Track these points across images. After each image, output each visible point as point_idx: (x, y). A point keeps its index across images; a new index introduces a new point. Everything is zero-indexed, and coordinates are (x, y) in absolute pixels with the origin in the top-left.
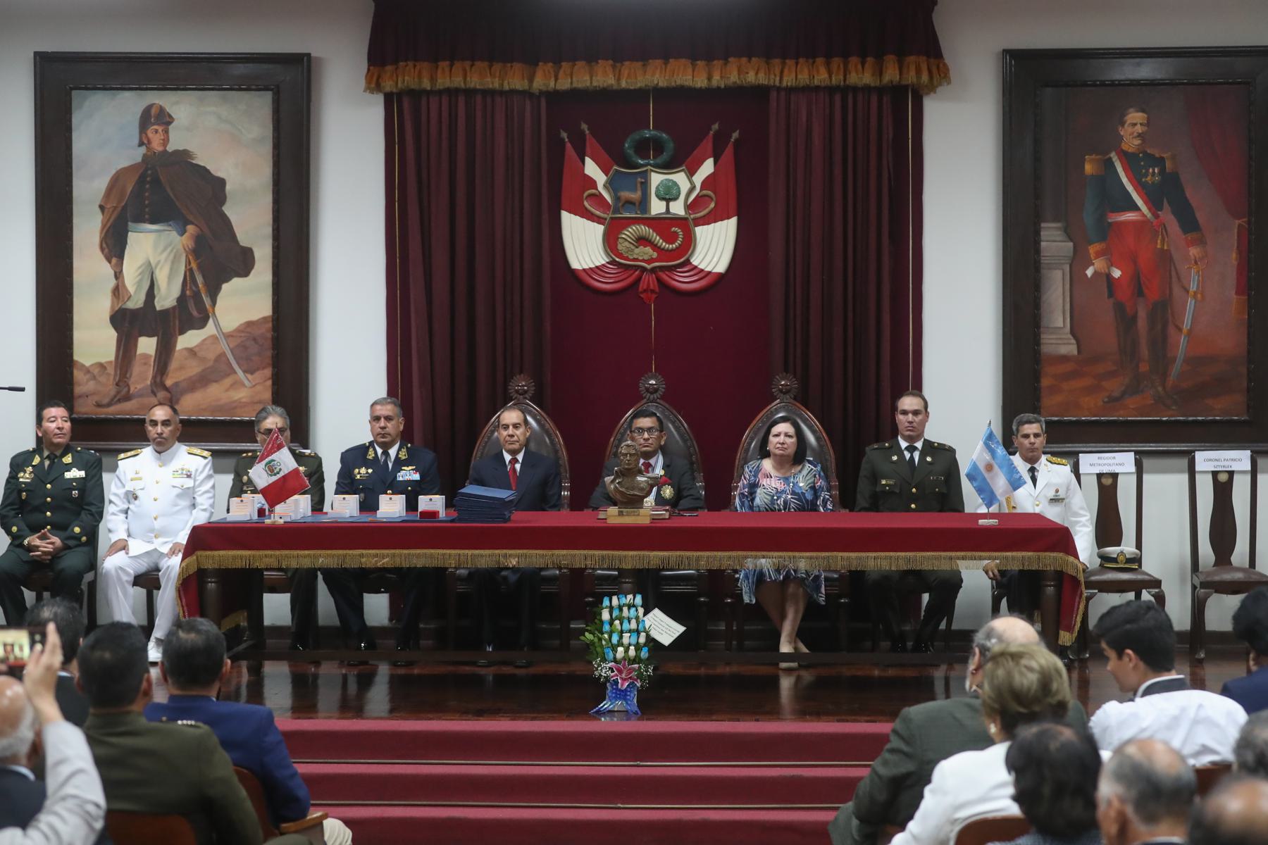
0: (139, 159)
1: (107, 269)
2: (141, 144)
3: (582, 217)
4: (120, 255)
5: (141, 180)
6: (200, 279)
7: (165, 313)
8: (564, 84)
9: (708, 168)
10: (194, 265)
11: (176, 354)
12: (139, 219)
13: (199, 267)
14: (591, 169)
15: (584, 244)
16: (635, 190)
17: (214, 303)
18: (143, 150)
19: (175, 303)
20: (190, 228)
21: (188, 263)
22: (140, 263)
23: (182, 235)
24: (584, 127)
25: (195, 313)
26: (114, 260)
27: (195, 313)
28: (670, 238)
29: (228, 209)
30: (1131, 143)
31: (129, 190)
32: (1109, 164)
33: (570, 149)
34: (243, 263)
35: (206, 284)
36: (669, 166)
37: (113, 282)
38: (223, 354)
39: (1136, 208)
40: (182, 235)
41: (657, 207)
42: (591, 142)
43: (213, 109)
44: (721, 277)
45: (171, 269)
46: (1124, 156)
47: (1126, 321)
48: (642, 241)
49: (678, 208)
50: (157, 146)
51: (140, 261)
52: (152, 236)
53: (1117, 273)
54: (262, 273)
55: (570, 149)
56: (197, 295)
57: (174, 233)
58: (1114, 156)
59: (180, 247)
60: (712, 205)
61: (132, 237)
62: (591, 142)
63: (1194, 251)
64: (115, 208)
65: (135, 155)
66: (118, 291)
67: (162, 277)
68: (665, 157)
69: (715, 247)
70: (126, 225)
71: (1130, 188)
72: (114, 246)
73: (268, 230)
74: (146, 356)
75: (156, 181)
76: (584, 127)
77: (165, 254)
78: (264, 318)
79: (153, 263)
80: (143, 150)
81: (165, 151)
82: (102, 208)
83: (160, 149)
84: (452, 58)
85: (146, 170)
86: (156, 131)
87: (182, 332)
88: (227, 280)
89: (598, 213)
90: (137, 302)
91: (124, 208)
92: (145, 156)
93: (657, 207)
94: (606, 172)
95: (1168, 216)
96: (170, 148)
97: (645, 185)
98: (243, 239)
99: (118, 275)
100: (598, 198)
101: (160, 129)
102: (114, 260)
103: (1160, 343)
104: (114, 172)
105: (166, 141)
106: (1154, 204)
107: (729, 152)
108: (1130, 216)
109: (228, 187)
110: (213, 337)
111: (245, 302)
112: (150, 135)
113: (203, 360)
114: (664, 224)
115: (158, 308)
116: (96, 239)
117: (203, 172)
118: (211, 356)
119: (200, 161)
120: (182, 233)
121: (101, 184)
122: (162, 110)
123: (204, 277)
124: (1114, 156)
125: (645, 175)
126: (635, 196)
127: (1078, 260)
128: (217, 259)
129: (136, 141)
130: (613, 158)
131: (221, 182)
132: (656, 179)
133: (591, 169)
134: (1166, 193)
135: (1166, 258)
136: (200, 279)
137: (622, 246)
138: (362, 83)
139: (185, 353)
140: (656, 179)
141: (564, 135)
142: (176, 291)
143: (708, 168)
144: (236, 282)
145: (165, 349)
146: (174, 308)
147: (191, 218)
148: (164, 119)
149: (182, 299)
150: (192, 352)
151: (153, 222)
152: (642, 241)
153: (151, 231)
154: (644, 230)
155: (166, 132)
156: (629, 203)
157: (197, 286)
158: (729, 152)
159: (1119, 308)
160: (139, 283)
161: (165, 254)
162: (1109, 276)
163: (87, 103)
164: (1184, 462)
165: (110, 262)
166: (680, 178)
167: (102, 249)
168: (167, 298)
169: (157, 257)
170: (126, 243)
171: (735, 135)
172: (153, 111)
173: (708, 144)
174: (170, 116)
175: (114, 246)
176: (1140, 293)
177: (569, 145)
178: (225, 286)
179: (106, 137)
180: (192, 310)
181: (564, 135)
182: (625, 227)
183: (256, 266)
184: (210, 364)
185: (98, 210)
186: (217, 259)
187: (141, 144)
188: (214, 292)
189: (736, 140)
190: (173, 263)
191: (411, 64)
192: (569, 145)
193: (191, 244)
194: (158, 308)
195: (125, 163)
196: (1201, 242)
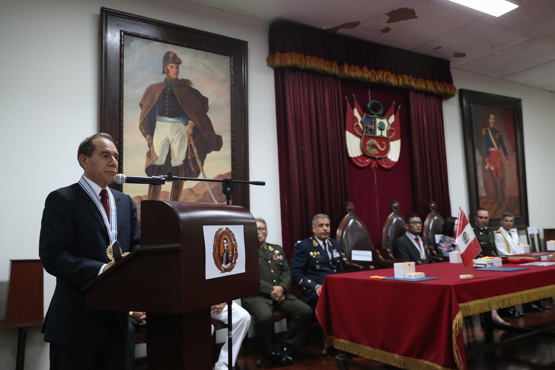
0: (163, 81)
1: (143, 141)
2: (164, 72)
3: (353, 134)
4: (152, 134)
5: (164, 92)
7: (177, 168)
8: (353, 74)
9: (392, 119)
10: (192, 143)
11: (183, 192)
12: (163, 114)
13: (196, 144)
14: (356, 113)
15: (354, 146)
16: (372, 124)
17: (203, 164)
18: (165, 76)
19: (182, 163)
20: (190, 122)
22: (163, 139)
23: (186, 125)
24: (354, 95)
25: (193, 169)
26: (148, 136)
27: (193, 169)
28: (382, 147)
29: (210, 114)
30: (492, 125)
31: (157, 96)
32: (487, 131)
33: (349, 105)
34: (217, 144)
35: (199, 153)
36: (382, 116)
37: (147, 149)
38: (208, 192)
39: (494, 147)
40: (186, 125)
41: (378, 133)
42: (356, 103)
43: (202, 60)
44: (396, 163)
45: (180, 144)
46: (491, 129)
47: (496, 185)
48: (374, 146)
49: (385, 134)
53: (492, 168)
54: (226, 150)
55: (349, 105)
56: (194, 159)
57: (182, 125)
58: (488, 129)
59: (185, 132)
60: (394, 134)
61: (158, 124)
62: (356, 103)
63: (507, 162)
64: (149, 107)
65: (162, 78)
66: (150, 154)
68: (381, 112)
69: (394, 152)
70: (155, 117)
71: (493, 140)
72: (148, 128)
73: (229, 127)
74: (166, 193)
75: (172, 94)
76: (354, 95)
77: (177, 135)
78: (228, 173)
79: (170, 141)
80: (165, 76)
81: (177, 79)
82: (141, 105)
83: (175, 77)
84: (312, 56)
85: (166, 87)
86: (172, 67)
89: (358, 133)
90: (161, 161)
91: (154, 107)
92: (166, 80)
93: (378, 133)
94: (362, 116)
95: (501, 150)
96: (180, 77)
97: (375, 122)
98: (217, 130)
99: (150, 145)
100: (358, 126)
101: (174, 66)
102: (148, 136)
103: (503, 192)
104: (148, 86)
105: (177, 73)
106: (498, 146)
107: (398, 112)
108: (493, 149)
109: (209, 103)
111: (217, 164)
112: (169, 67)
113: (197, 195)
114: (380, 139)
115: (173, 165)
116: (138, 123)
117: (196, 93)
118: (201, 193)
119: (196, 86)
120: (186, 124)
121: (141, 92)
122: (175, 56)
123: (198, 150)
124: (488, 129)
125: (374, 118)
126: (372, 127)
127: (484, 164)
128: (204, 141)
129: (161, 70)
130: (364, 110)
131: (205, 100)
132: (378, 121)
133: (356, 113)
134: (500, 142)
135: (502, 164)
137: (368, 148)
138: (265, 63)
139: (188, 191)
140: (378, 121)
141: (346, 98)
142: (183, 157)
143: (392, 119)
144: (214, 153)
145: (177, 189)
146: (182, 166)
147: (190, 116)
149: (186, 161)
150: (191, 190)
151: (170, 117)
152: (374, 146)
154: (375, 142)
155: (178, 68)
156: (371, 130)
157: (194, 154)
158: (398, 112)
159: (494, 180)
160: (162, 151)
161: (177, 135)
162: (490, 169)
164: (524, 231)
165: (145, 137)
166: (385, 121)
167: (141, 130)
168: (178, 160)
169: (171, 135)
170: (155, 127)
171: (399, 107)
172: (171, 56)
173: (392, 109)
174: (180, 60)
175: (148, 128)
176: (497, 175)
177: (348, 103)
178: (208, 155)
179: (144, 66)
180: (191, 168)
181: (346, 98)
182: (370, 139)
183: (223, 146)
184: (201, 197)
185: (139, 106)
186: (204, 141)
187: (164, 72)
188: (203, 159)
189: (401, 109)
190: (181, 140)
191: (296, 54)
192: (348, 103)
193: (191, 131)
194: (173, 165)
195: (154, 82)
196: (508, 159)
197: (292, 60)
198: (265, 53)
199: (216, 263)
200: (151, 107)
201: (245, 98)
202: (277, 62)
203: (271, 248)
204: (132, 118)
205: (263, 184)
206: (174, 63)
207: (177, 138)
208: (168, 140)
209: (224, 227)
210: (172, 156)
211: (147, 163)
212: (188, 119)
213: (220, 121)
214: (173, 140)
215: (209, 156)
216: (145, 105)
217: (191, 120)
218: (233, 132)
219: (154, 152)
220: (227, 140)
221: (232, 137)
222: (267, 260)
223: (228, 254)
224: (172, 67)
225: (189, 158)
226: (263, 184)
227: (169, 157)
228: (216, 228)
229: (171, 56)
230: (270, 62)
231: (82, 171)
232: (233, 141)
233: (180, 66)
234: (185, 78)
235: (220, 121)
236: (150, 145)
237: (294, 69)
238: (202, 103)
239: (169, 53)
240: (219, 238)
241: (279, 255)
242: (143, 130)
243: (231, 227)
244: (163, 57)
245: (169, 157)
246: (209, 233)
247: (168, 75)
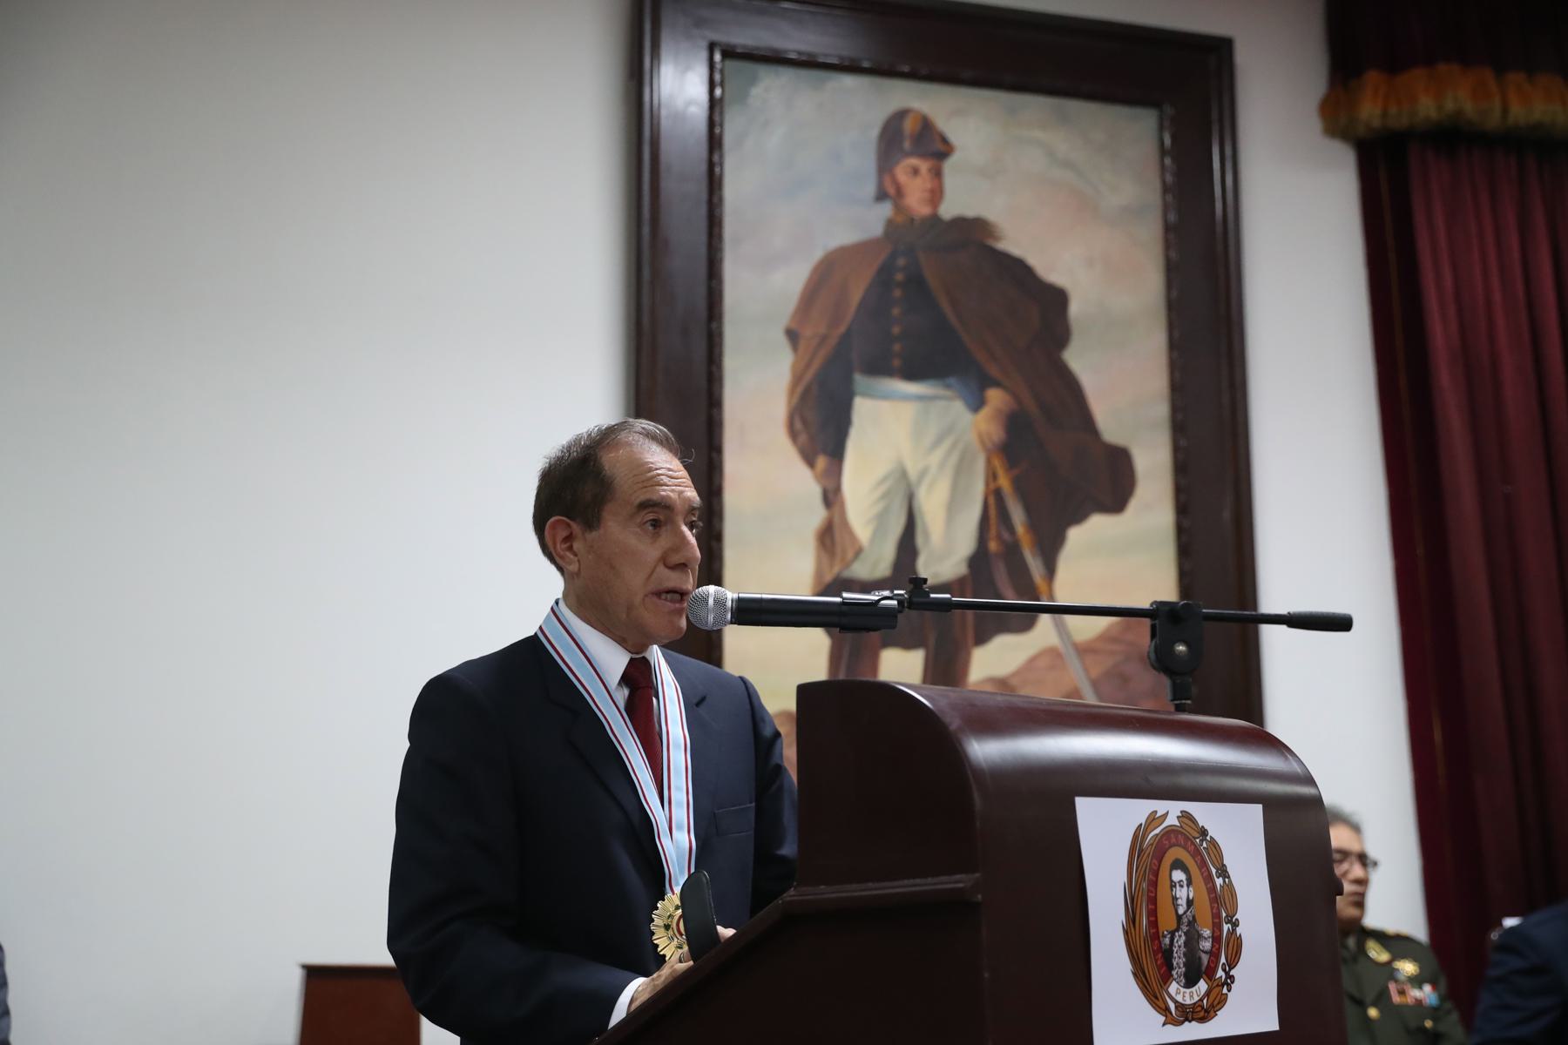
1: (803, 482)
2: (881, 196)
4: (836, 453)
6: (1018, 516)
10: (1004, 482)
12: (879, 367)
18: (886, 210)
19: (962, 570)
20: (995, 397)
21: (991, 476)
26: (821, 462)
29: (1077, 359)
31: (856, 295)
34: (1109, 483)
35: (1033, 525)
37: (818, 515)
50: (916, 201)
51: (882, 467)
52: (908, 411)
54: (1152, 507)
56: (1012, 552)
57: (958, 408)
59: (972, 438)
61: (862, 408)
64: (824, 339)
65: (871, 221)
66: (831, 536)
67: (932, 506)
72: (822, 428)
73: (1162, 410)
75: (916, 283)
79: (913, 473)
80: (886, 210)
81: (935, 219)
82: (792, 335)
83: (925, 211)
85: (893, 256)
86: (916, 171)
87: (982, 639)
88: (1079, 517)
91: (847, 336)
92: (890, 224)
96: (948, 210)
99: (831, 496)
101: (924, 166)
102: (821, 462)
104: (818, 254)
105: (936, 195)
109: (1075, 309)
110: (1052, 653)
112: (901, 172)
116: (777, 406)
117: (1018, 272)
119: (1014, 242)
120: (977, 404)
121: (791, 280)
122: (926, 126)
123: (1029, 510)
128: (1054, 470)
129: (870, 188)
131: (1056, 299)
136: (1018, 516)
138: (1315, 124)
142: (965, 543)
144: (1098, 524)
147: (993, 371)
148: (934, 147)
149: (979, 561)
151: (911, 375)
153: (906, 398)
155: (937, 174)
157: (1011, 528)
160: (881, 520)
163: (756, 91)
165: (810, 463)
167: (793, 434)
168: (946, 556)
169: (918, 455)
172: (909, 125)
174: (944, 140)
175: (822, 428)
180: (1003, 588)
187: (881, 196)
188: (1050, 548)
193: (996, 433)
197: (1436, 97)
198: (1313, 80)
199: (1140, 974)
200: (833, 341)
201: (1227, 267)
202: (1370, 112)
203: (1378, 954)
204: (757, 389)
205: (1341, 624)
206: (923, 155)
207: (942, 465)
208: (903, 474)
209: (1172, 810)
210: (920, 540)
211: (819, 574)
212: (985, 382)
213: (1123, 383)
214: (923, 473)
215: (1077, 536)
216: (808, 332)
217: (997, 384)
218: (1179, 428)
219: (845, 524)
220: (1153, 464)
221: (1176, 449)
222: (1361, 1005)
223: (1193, 938)
224: (916, 171)
225: (993, 546)
226: (1341, 624)
227: (908, 546)
228: (1139, 810)
229: (909, 125)
230: (1336, 116)
231: (551, 584)
232: (1183, 468)
233: (948, 166)
234: (970, 213)
235: (1123, 383)
236: (831, 496)
237: (1451, 138)
238: (1045, 310)
239: (901, 115)
240: (1149, 858)
241: (1417, 981)
242: (803, 438)
243: (1203, 813)
244: (875, 133)
245: (908, 546)
246: (1105, 833)
247: (898, 208)
